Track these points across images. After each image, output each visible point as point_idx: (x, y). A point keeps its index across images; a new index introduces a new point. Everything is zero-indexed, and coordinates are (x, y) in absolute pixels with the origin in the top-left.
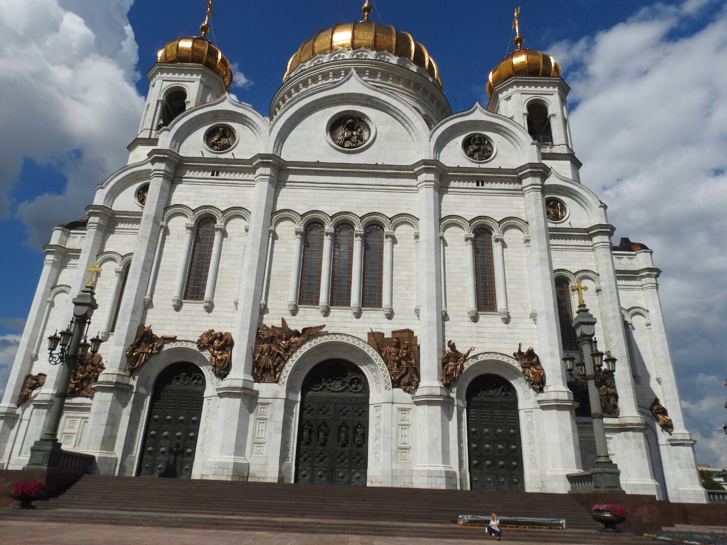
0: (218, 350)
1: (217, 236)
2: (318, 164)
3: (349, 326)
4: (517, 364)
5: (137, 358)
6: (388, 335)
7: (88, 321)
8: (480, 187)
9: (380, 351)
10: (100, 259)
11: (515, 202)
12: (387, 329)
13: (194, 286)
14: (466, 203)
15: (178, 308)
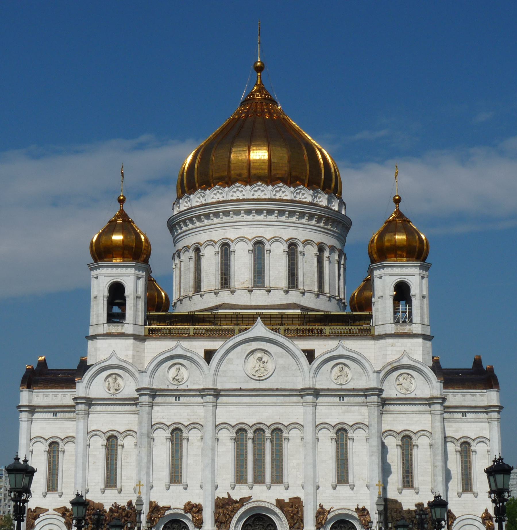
0: (195, 513)
1: (185, 443)
2: (241, 390)
3: (265, 496)
4: (356, 515)
5: (154, 520)
6: (287, 501)
7: (142, 512)
8: (342, 401)
9: (282, 511)
10: (89, 436)
11: (363, 411)
12: (286, 496)
13: (176, 476)
14: (333, 413)
15: (168, 489)
